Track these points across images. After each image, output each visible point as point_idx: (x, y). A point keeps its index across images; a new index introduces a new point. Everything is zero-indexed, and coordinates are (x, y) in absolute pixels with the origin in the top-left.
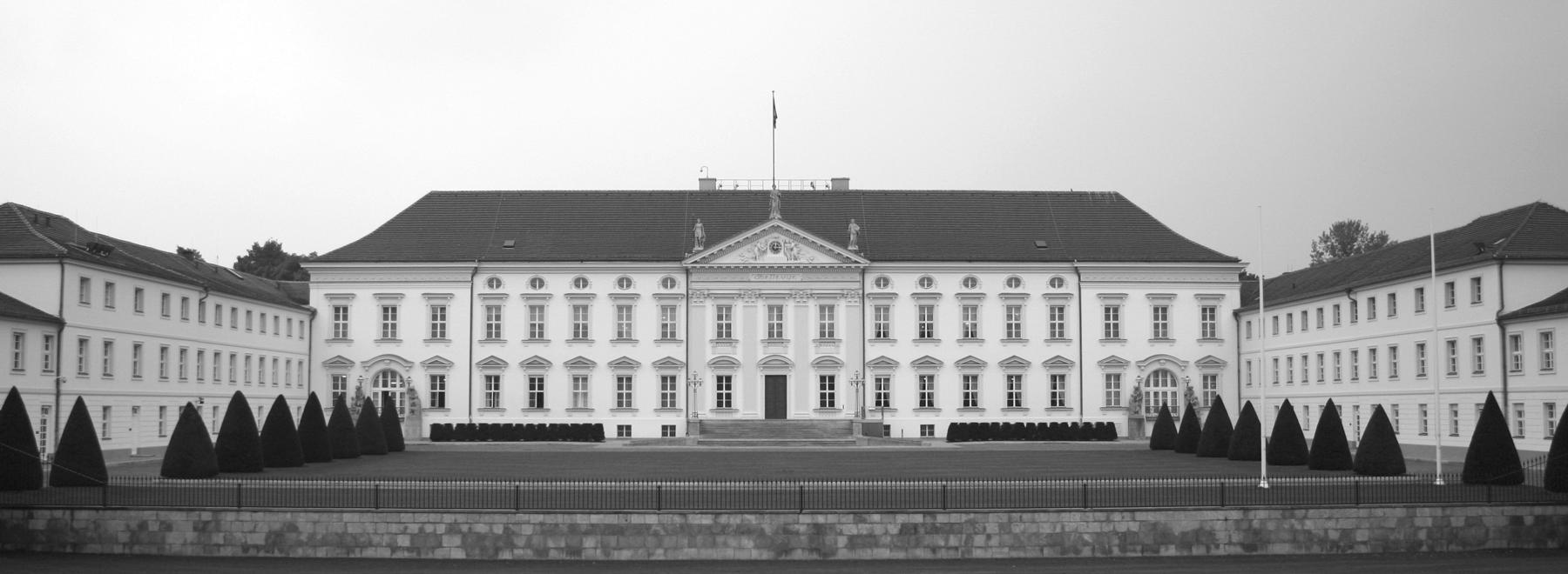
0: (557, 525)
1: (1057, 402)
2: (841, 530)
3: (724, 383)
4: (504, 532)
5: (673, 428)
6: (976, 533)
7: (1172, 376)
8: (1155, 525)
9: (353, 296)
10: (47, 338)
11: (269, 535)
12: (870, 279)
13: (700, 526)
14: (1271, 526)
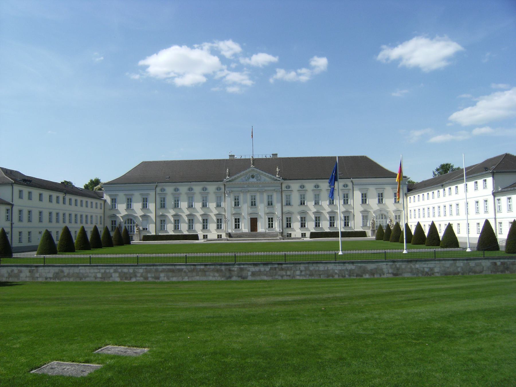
0: (151, 269)
1: (346, 224)
2: (249, 269)
3: (237, 221)
4: (133, 272)
5: (221, 235)
6: (297, 270)
7: (385, 216)
8: (360, 267)
9: (118, 195)
10: (8, 210)
11: (54, 273)
12: (284, 186)
13: (200, 269)
14: (403, 266)
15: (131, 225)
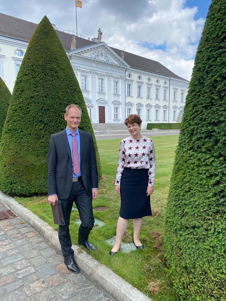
12: (127, 73)
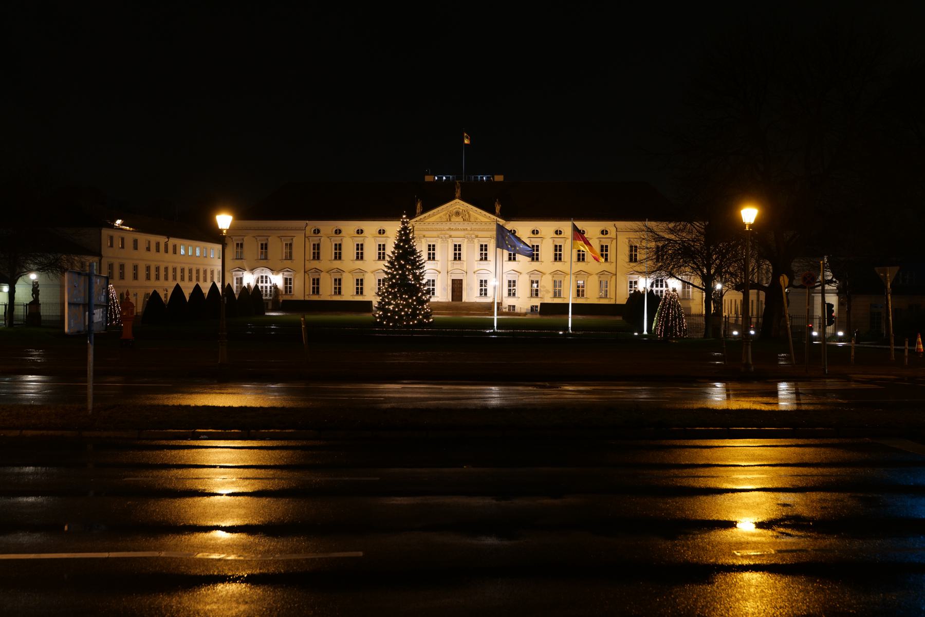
7: (666, 282)
15: (266, 285)
